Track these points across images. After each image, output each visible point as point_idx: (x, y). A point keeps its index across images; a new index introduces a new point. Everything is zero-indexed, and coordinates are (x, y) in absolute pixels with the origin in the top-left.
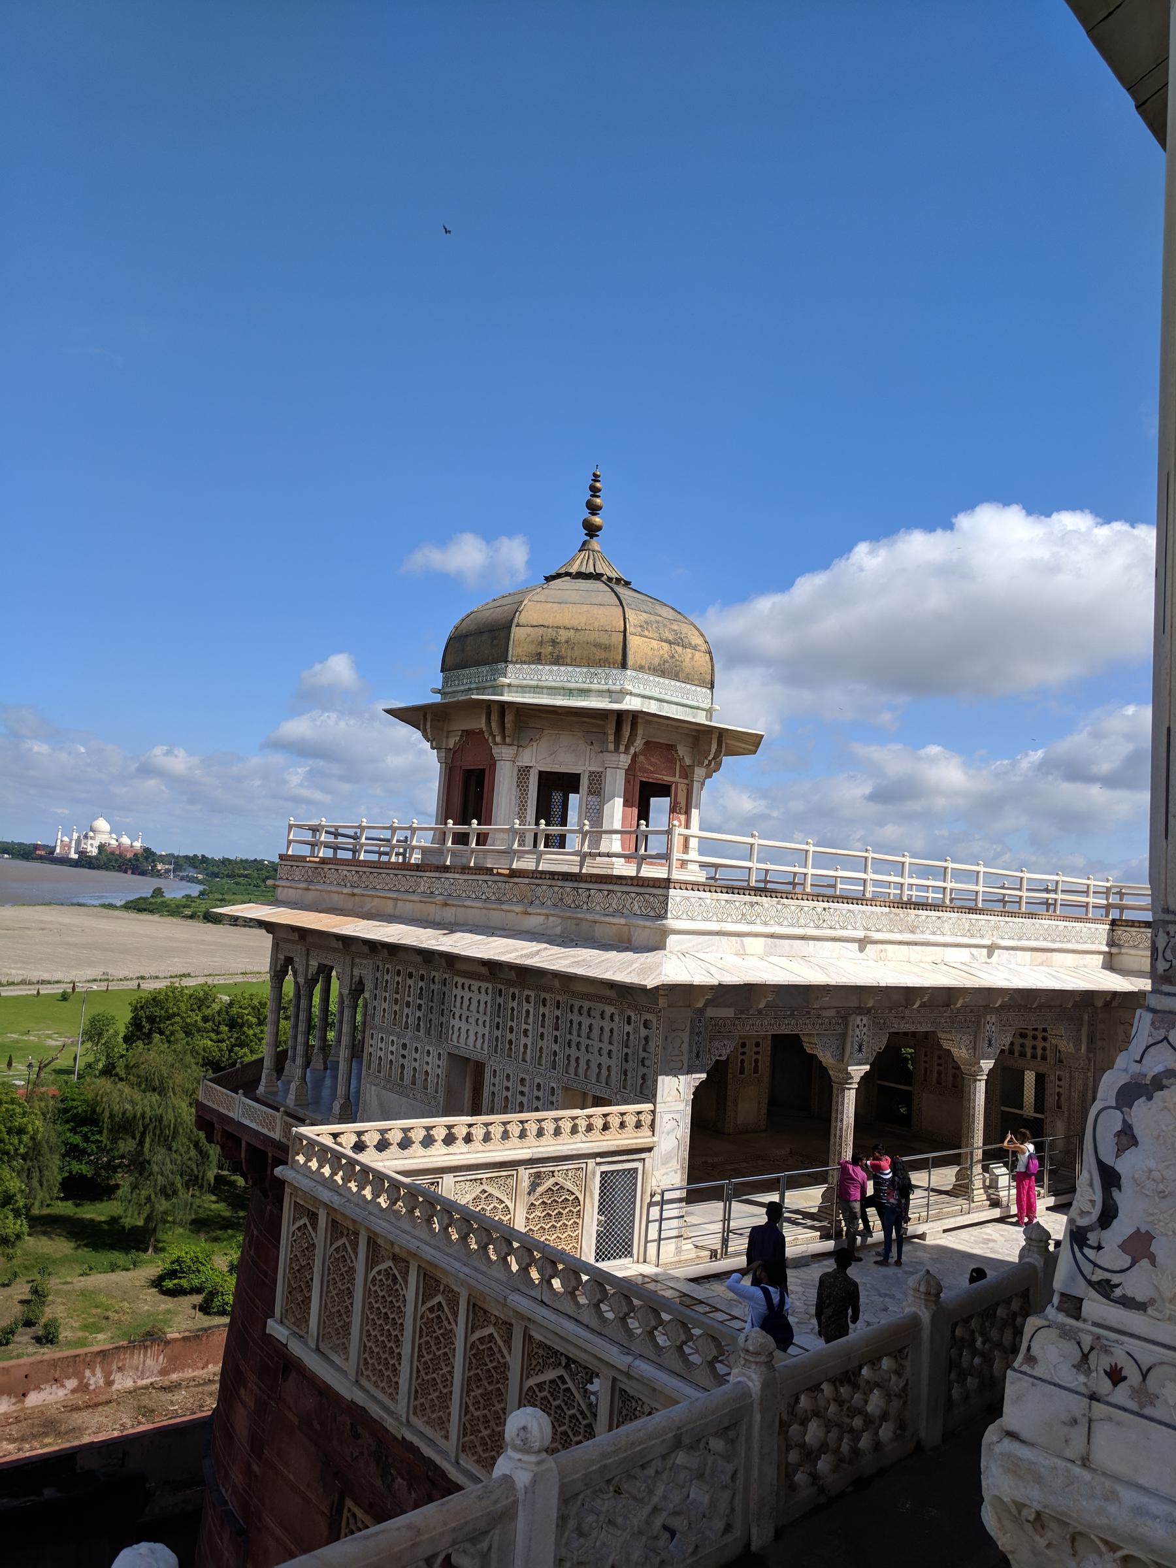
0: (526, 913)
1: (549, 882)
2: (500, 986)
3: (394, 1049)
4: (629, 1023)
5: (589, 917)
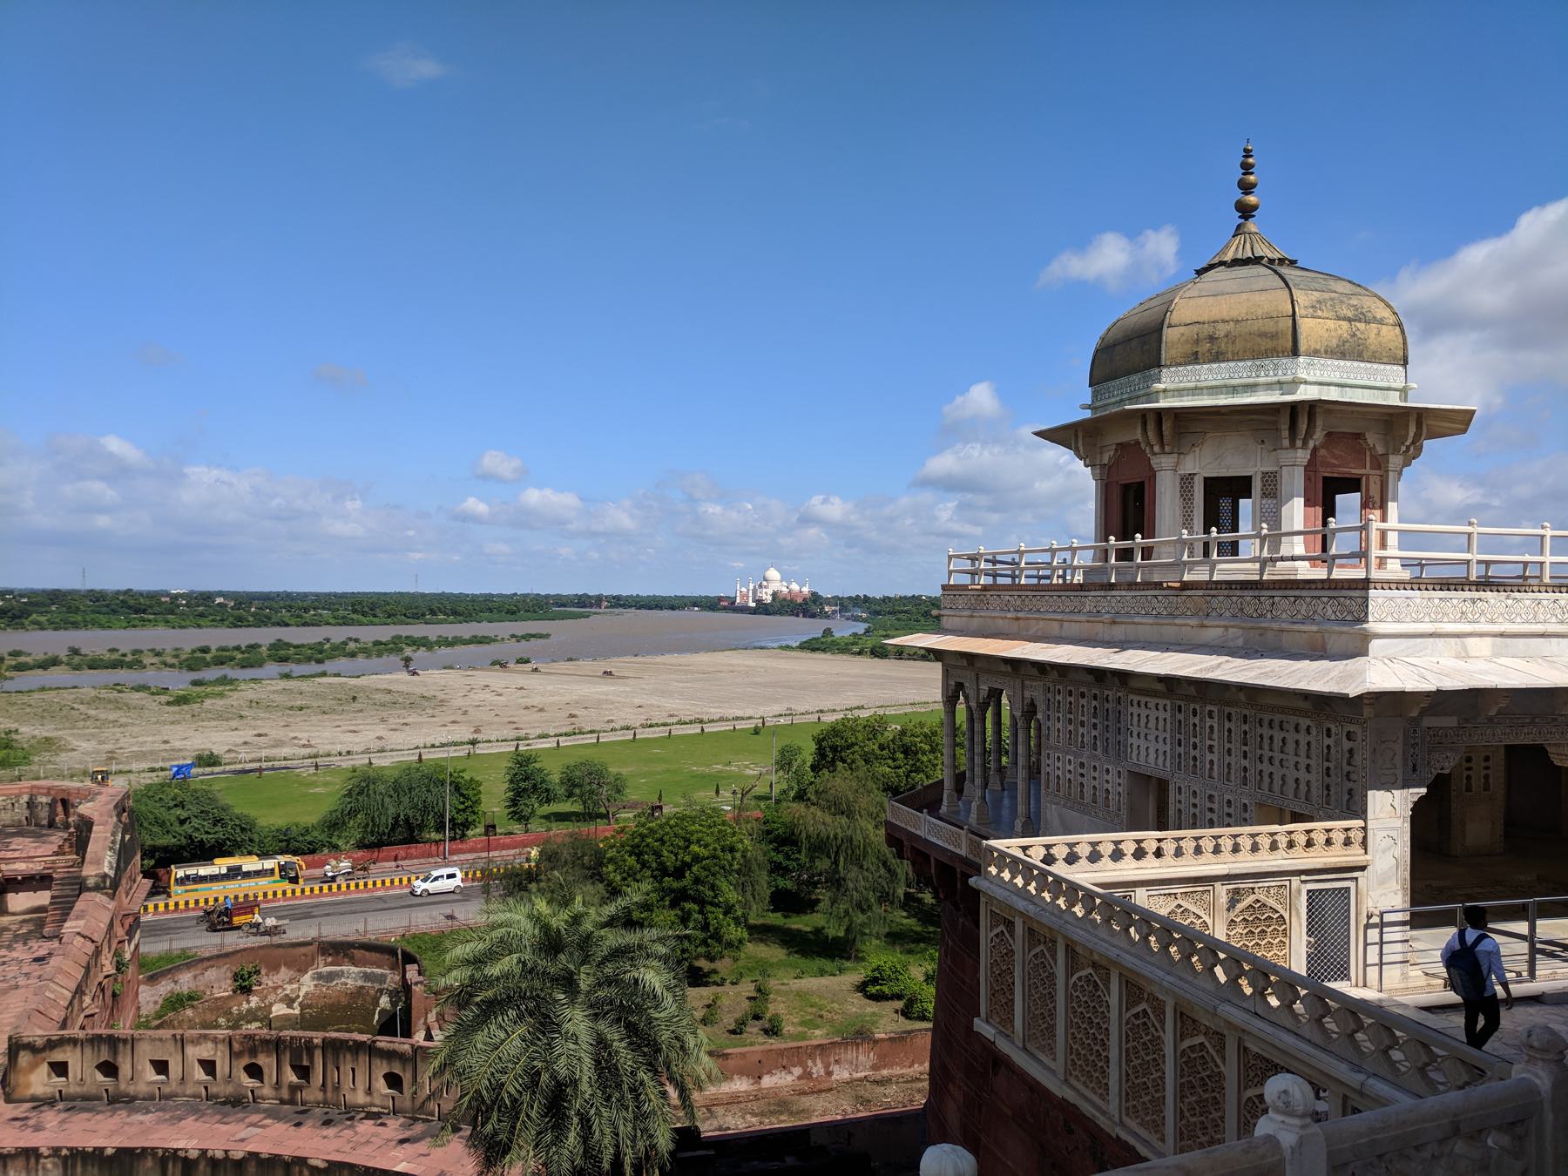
0: (1203, 626)
4: (1329, 736)
5: (1275, 626)
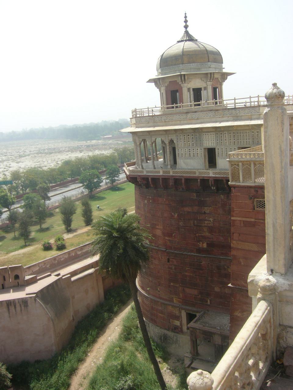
0: (223, 117)
1: (228, 110)
2: (217, 133)
3: (186, 151)
4: (253, 133)
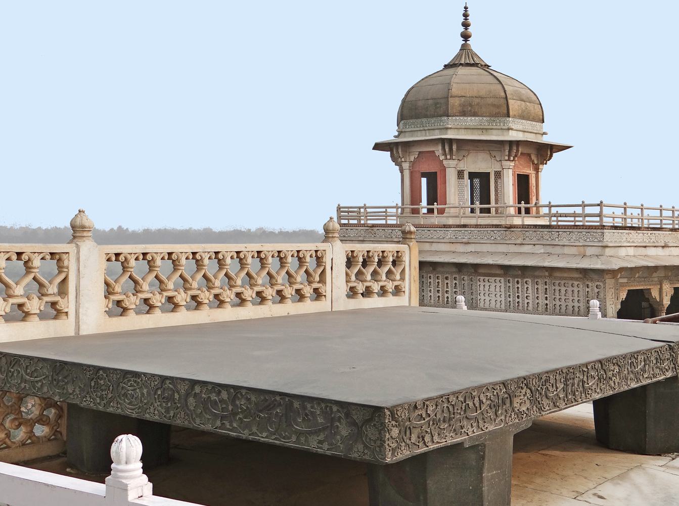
1: (534, 230)
2: (508, 279)
4: (588, 287)
